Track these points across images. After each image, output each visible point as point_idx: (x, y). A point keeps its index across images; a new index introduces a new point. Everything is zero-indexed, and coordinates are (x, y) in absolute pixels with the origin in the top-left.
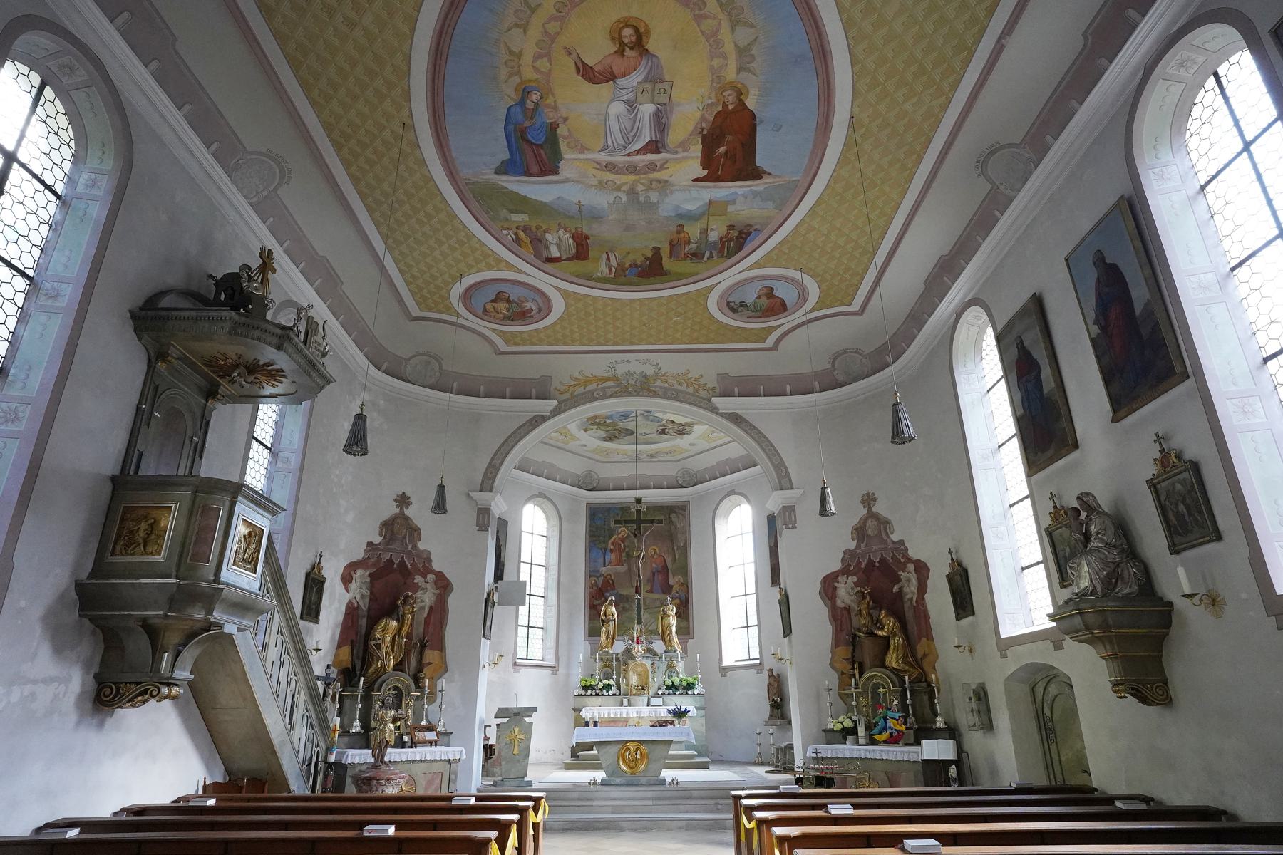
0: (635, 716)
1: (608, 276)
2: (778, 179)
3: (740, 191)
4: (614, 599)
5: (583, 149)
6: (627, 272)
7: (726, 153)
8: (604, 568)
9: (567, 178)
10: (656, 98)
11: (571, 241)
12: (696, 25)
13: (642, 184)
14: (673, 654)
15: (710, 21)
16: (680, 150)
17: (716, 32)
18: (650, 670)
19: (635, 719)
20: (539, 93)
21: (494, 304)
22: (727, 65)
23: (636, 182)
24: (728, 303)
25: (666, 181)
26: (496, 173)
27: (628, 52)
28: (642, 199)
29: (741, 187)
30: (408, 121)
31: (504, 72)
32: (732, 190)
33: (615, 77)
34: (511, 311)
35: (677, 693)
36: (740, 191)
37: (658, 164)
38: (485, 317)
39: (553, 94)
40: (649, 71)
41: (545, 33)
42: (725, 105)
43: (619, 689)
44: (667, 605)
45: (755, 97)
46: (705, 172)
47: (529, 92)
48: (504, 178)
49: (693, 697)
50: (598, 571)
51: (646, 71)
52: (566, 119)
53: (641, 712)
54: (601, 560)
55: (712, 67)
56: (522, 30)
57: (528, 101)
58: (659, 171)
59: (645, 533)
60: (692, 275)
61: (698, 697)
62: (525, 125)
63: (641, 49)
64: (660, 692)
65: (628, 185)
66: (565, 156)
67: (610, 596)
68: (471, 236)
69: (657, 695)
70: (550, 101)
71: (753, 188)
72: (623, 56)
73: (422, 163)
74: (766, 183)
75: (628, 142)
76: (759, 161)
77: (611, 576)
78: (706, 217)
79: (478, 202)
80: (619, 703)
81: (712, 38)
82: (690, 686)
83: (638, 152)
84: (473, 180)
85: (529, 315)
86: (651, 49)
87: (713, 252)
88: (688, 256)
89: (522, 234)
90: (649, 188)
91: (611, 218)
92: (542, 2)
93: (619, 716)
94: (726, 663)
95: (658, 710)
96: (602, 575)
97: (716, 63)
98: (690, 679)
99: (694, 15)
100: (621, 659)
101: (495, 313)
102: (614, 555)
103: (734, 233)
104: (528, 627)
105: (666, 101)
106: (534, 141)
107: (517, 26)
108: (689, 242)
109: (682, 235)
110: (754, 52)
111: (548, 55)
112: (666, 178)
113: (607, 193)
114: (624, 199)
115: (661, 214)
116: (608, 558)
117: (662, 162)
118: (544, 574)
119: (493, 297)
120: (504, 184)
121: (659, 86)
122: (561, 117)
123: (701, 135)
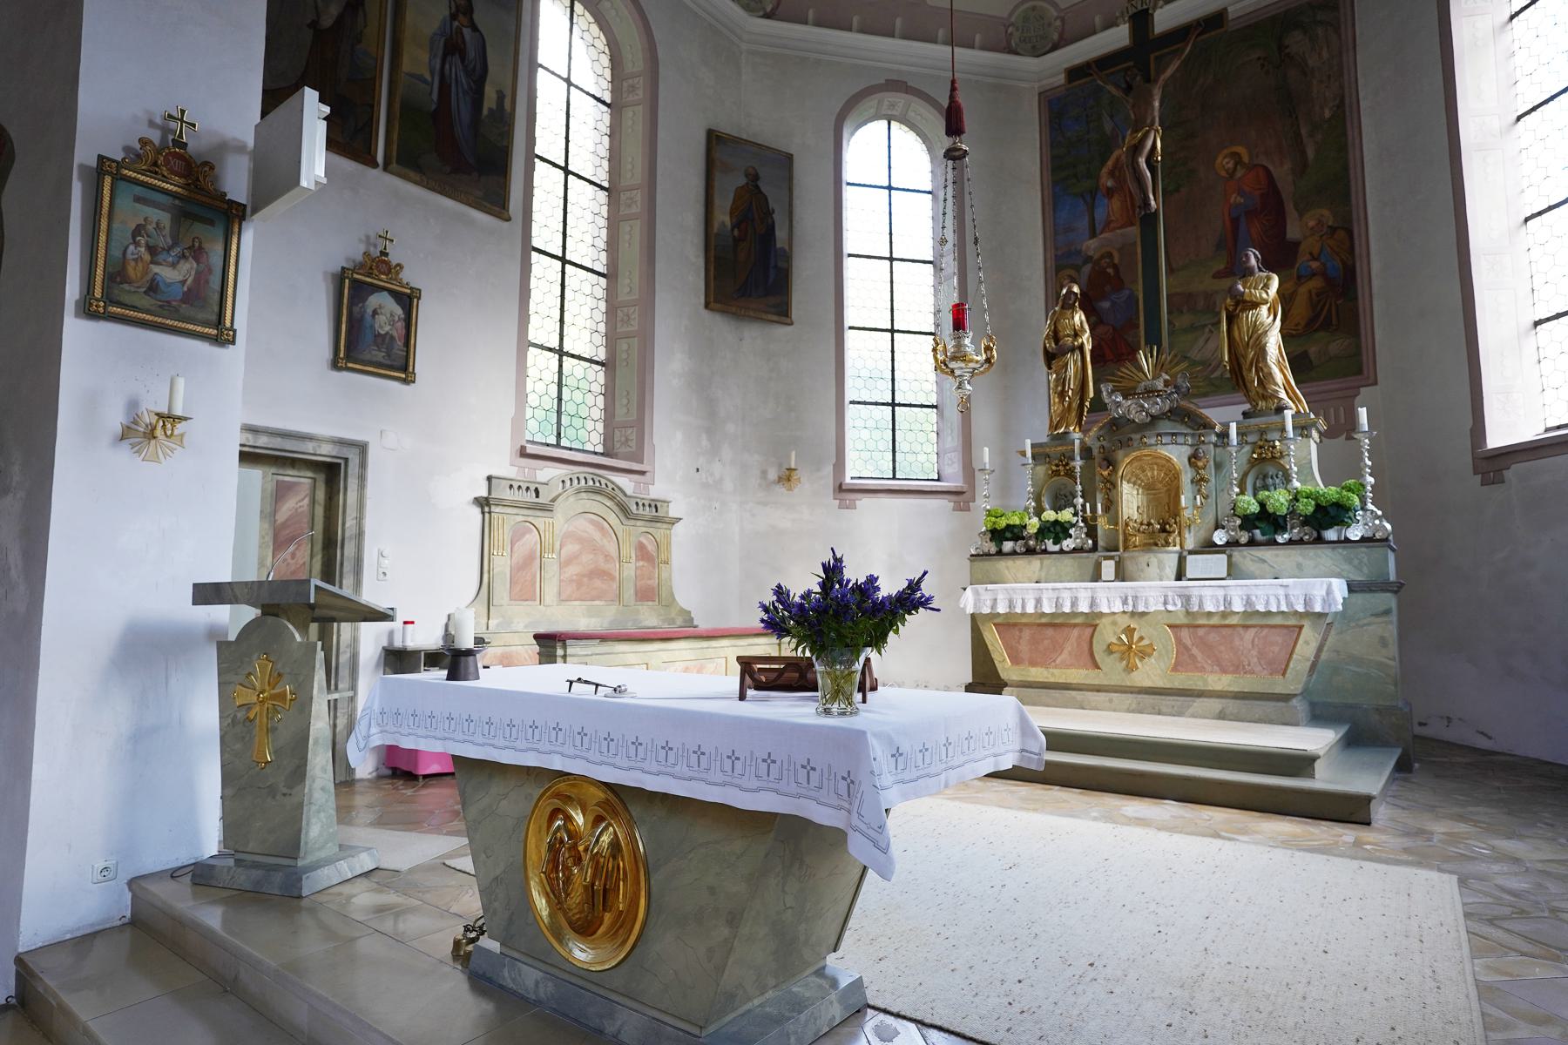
0: (1118, 607)
4: (1076, 289)
8: (1091, 241)
14: (1275, 419)
18: (1186, 477)
19: (1119, 619)
35: (1280, 539)
43: (1092, 532)
44: (1247, 273)
49: (1341, 551)
50: (1079, 252)
53: (1135, 598)
54: (1083, 224)
59: (1160, 71)
61: (1363, 550)
64: (1220, 538)
67: (1074, 281)
69: (1209, 547)
77: (1110, 255)
80: (1090, 569)
82: (1328, 515)
93: (1067, 609)
94: (1496, 438)
95: (1195, 593)
96: (1088, 259)
98: (1332, 492)
100: (1095, 452)
102: (1116, 203)
104: (893, 404)
116: (1100, 214)
118: (930, 280)
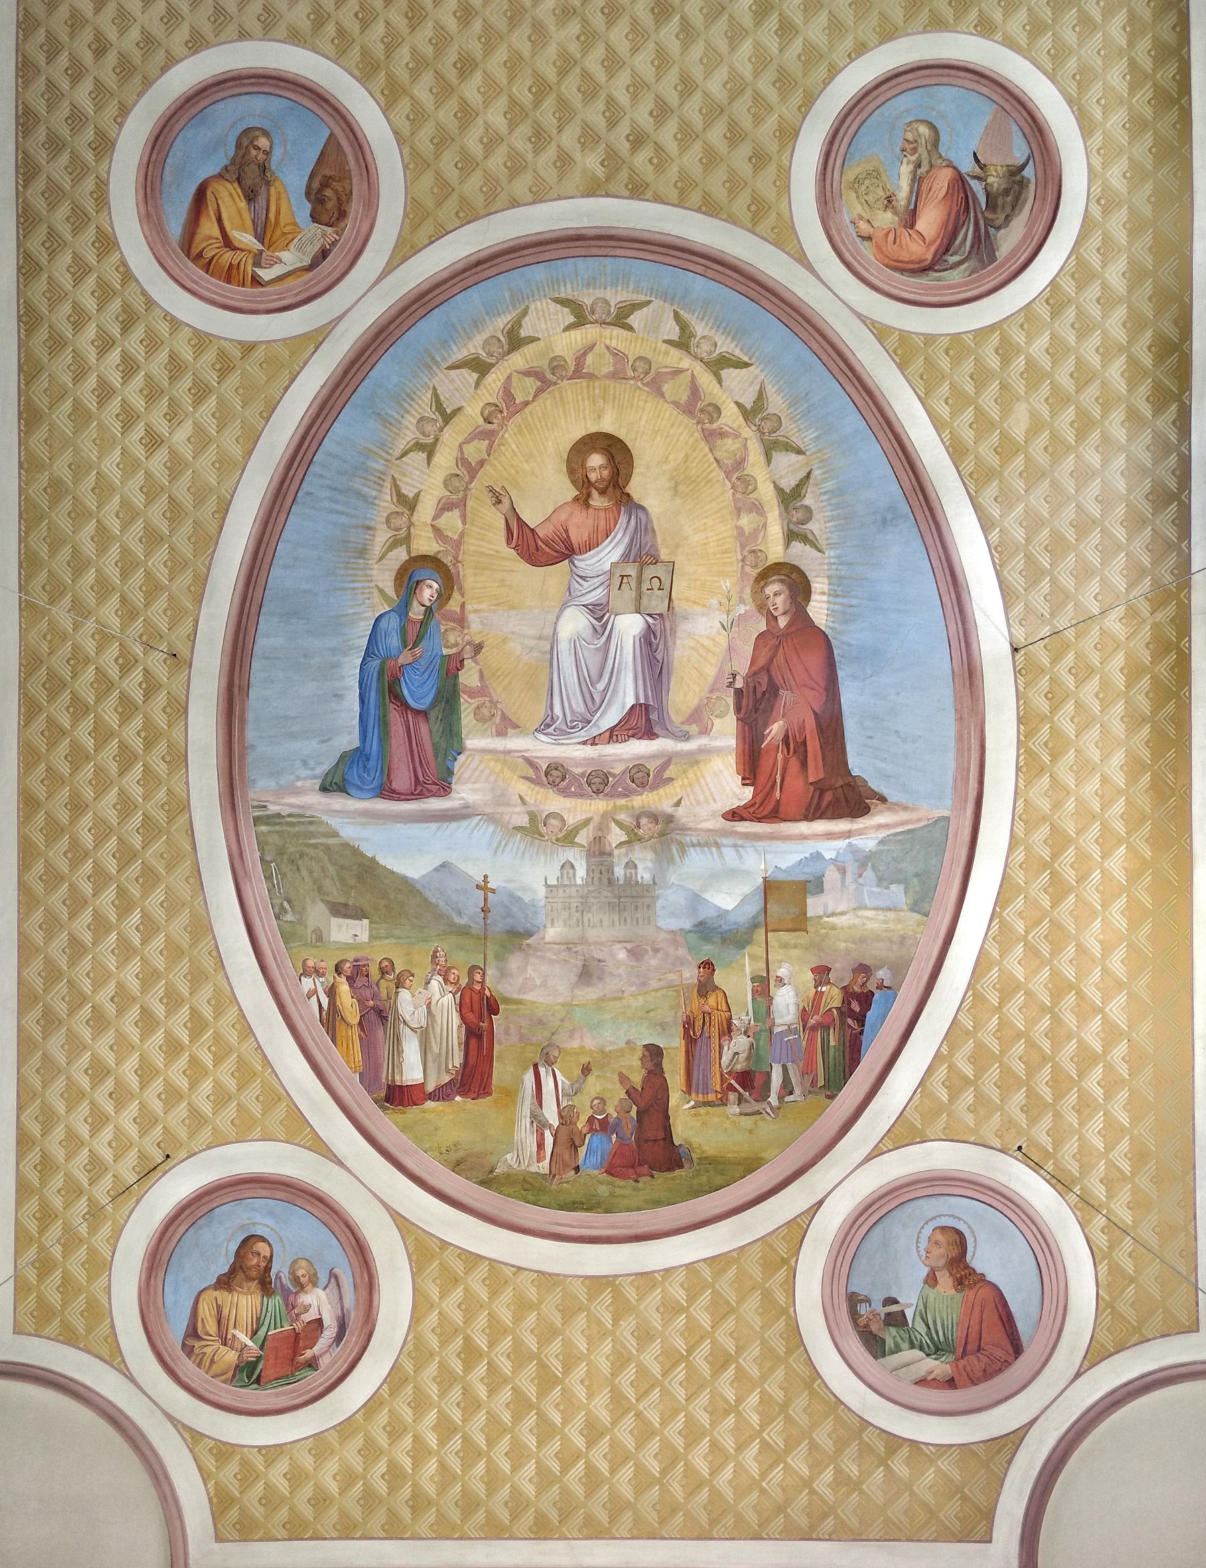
1: (533, 1169)
2: (904, 816)
3: (829, 850)
5: (506, 726)
6: (582, 1151)
7: (786, 740)
9: (467, 807)
10: (645, 601)
11: (456, 1020)
12: (707, 449)
13: (620, 824)
15: (729, 441)
16: (694, 729)
17: (740, 463)
20: (435, 586)
21: (223, 1296)
22: (765, 524)
23: (607, 817)
24: (853, 1300)
25: (670, 819)
26: (324, 789)
27: (597, 501)
28: (619, 871)
29: (830, 836)
30: (182, 649)
31: (382, 537)
32: (810, 848)
33: (574, 552)
34: (262, 1332)
36: (829, 850)
37: (652, 766)
38: (187, 1367)
39: (460, 589)
40: (632, 540)
41: (462, 461)
42: (772, 618)
45: (825, 598)
46: (748, 793)
47: (418, 583)
48: (338, 802)
51: (627, 540)
52: (478, 648)
55: (740, 531)
56: (424, 456)
57: (415, 603)
58: (655, 787)
60: (751, 1165)
62: (401, 661)
63: (618, 493)
65: (591, 826)
66: (470, 743)
68: (226, 999)
70: (453, 605)
71: (856, 841)
72: (588, 506)
73: (179, 759)
74: (880, 827)
75: (594, 706)
76: (858, 763)
78: (760, 934)
79: (269, 878)
81: (735, 469)
83: (612, 735)
84: (273, 808)
85: (308, 1354)
86: (635, 496)
87: (789, 1065)
88: (731, 1088)
89: (344, 988)
90: (634, 838)
91: (552, 933)
92: (464, 404)
97: (746, 521)
99: (703, 430)
101: (217, 1345)
103: (833, 997)
105: (662, 608)
106: (410, 701)
107: (418, 446)
108: (728, 1029)
109: (712, 1000)
110: (807, 501)
111: (461, 505)
112: (669, 810)
113: (545, 852)
114: (581, 872)
115: (661, 923)
117: (659, 762)
119: (223, 1265)
120: (334, 822)
121: (649, 572)
122: (469, 643)
123: (732, 690)
